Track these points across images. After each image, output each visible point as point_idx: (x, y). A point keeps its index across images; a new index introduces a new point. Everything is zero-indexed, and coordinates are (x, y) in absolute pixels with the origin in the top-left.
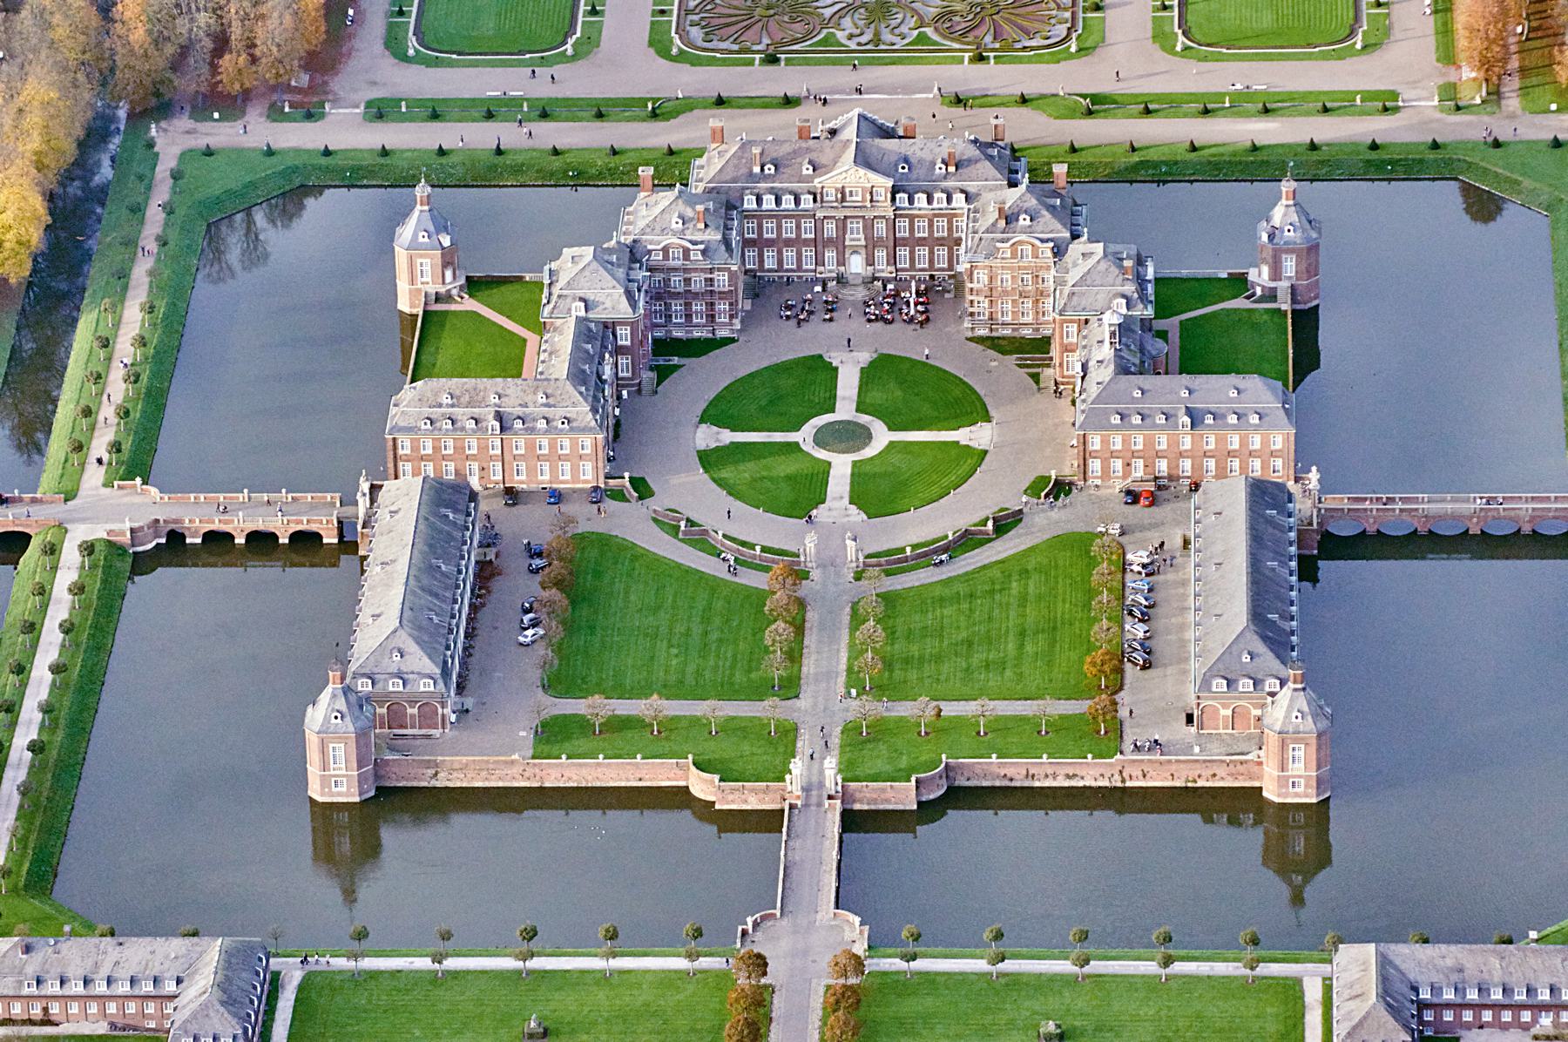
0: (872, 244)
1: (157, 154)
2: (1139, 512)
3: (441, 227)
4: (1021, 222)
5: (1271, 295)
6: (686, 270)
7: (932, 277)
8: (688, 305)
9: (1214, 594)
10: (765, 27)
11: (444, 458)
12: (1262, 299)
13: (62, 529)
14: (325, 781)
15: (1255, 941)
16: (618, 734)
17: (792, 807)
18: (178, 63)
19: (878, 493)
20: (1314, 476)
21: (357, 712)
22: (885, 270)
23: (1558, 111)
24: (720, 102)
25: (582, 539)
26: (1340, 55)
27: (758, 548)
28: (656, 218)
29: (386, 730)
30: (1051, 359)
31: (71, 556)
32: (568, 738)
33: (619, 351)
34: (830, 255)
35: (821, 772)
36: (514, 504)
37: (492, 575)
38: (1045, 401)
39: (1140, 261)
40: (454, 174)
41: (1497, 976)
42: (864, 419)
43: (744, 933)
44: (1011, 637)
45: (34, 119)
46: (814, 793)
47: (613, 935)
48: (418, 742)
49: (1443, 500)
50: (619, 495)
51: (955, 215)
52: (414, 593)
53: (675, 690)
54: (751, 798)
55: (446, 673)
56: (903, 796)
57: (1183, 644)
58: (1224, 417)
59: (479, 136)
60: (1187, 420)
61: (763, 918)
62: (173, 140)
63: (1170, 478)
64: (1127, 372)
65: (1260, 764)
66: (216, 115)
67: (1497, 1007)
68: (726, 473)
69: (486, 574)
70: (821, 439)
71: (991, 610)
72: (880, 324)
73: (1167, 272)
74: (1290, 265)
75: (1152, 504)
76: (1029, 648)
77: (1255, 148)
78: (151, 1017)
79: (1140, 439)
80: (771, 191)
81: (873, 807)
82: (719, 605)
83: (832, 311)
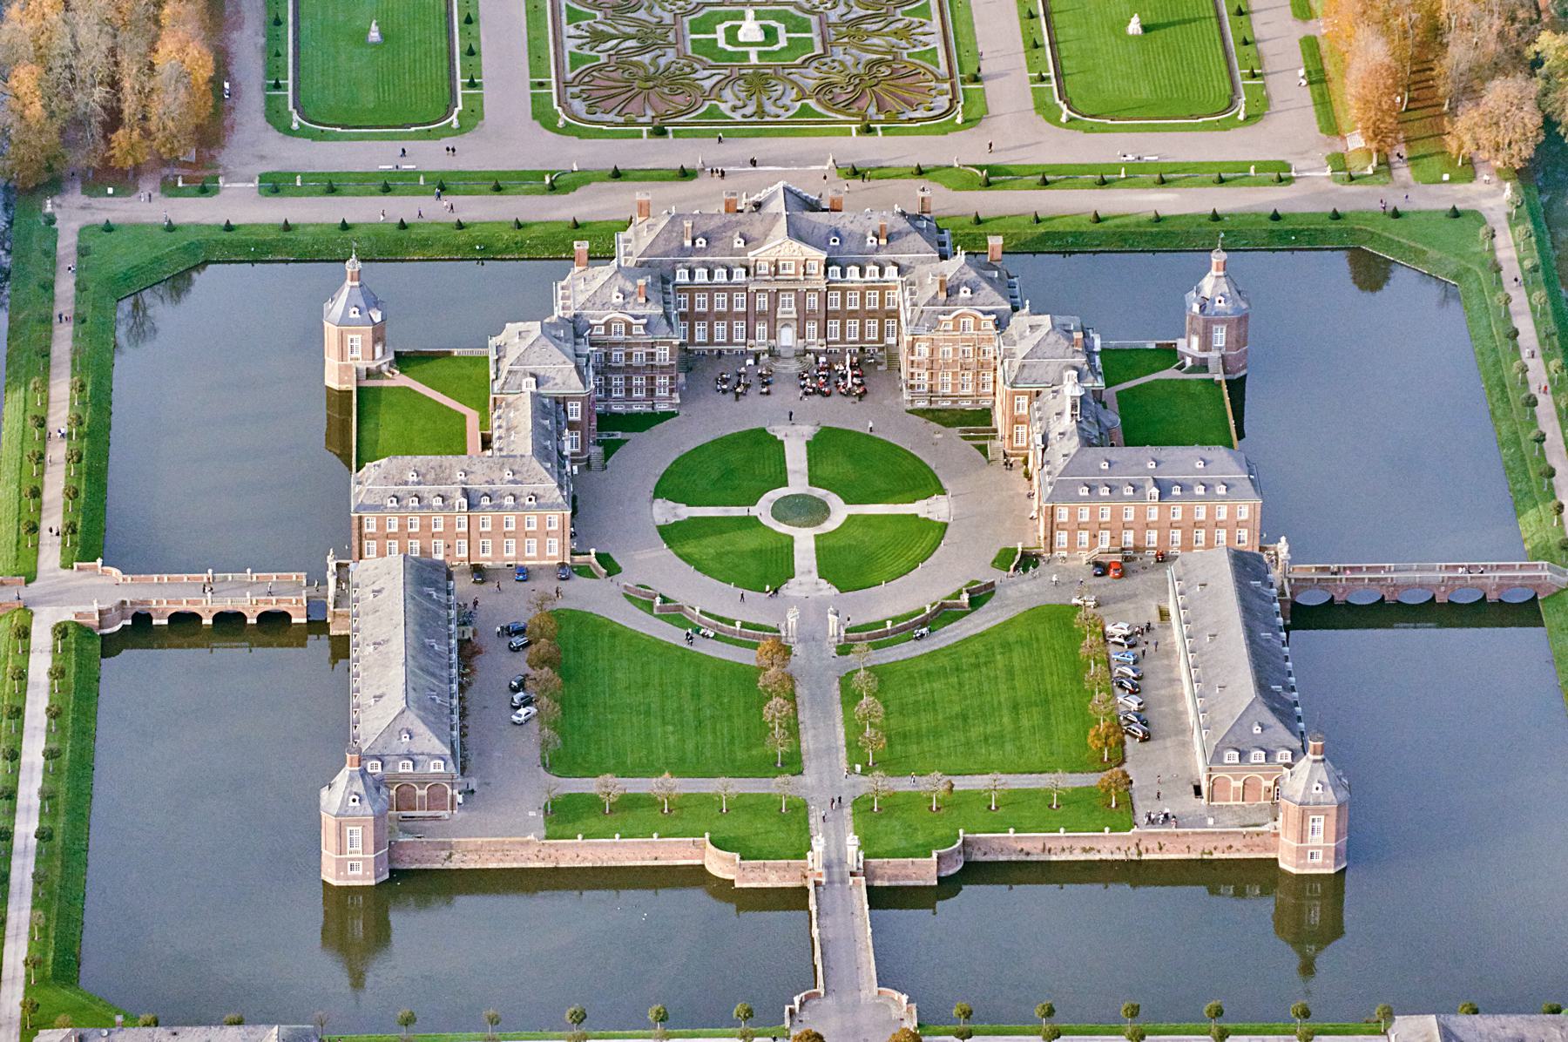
0: (803, 317)
1: (56, 231)
2: (1109, 583)
3: (372, 301)
4: (962, 294)
5: (1202, 366)
6: (628, 345)
7: (862, 349)
8: (628, 379)
10: (647, 98)
12: (1192, 370)
14: (340, 864)
15: (1306, 1014)
16: (631, 813)
17: (817, 884)
19: (846, 566)
20: (1282, 547)
21: (373, 791)
22: (814, 341)
23: (1451, 180)
24: (617, 175)
27: (738, 624)
28: (586, 289)
29: (394, 812)
30: (995, 431)
31: (42, 637)
32: (578, 818)
33: (572, 426)
35: (840, 846)
36: (482, 582)
37: (477, 652)
38: (995, 473)
42: (819, 492)
43: (792, 1012)
44: (1005, 712)
46: (836, 869)
48: (427, 824)
49: (1410, 570)
51: (888, 288)
52: (415, 674)
56: (925, 871)
57: (1179, 716)
58: (1191, 488)
60: (1155, 491)
61: (808, 997)
62: (72, 215)
63: (1136, 549)
64: (1092, 445)
65: (1276, 835)
66: (110, 191)
68: (690, 548)
69: (467, 652)
70: (779, 511)
71: (980, 683)
72: (817, 397)
73: (1113, 343)
74: (1220, 336)
75: (1122, 576)
76: (1025, 723)
77: (1158, 219)
79: (1108, 511)
80: (704, 264)
81: (894, 883)
82: (706, 681)
83: (767, 384)
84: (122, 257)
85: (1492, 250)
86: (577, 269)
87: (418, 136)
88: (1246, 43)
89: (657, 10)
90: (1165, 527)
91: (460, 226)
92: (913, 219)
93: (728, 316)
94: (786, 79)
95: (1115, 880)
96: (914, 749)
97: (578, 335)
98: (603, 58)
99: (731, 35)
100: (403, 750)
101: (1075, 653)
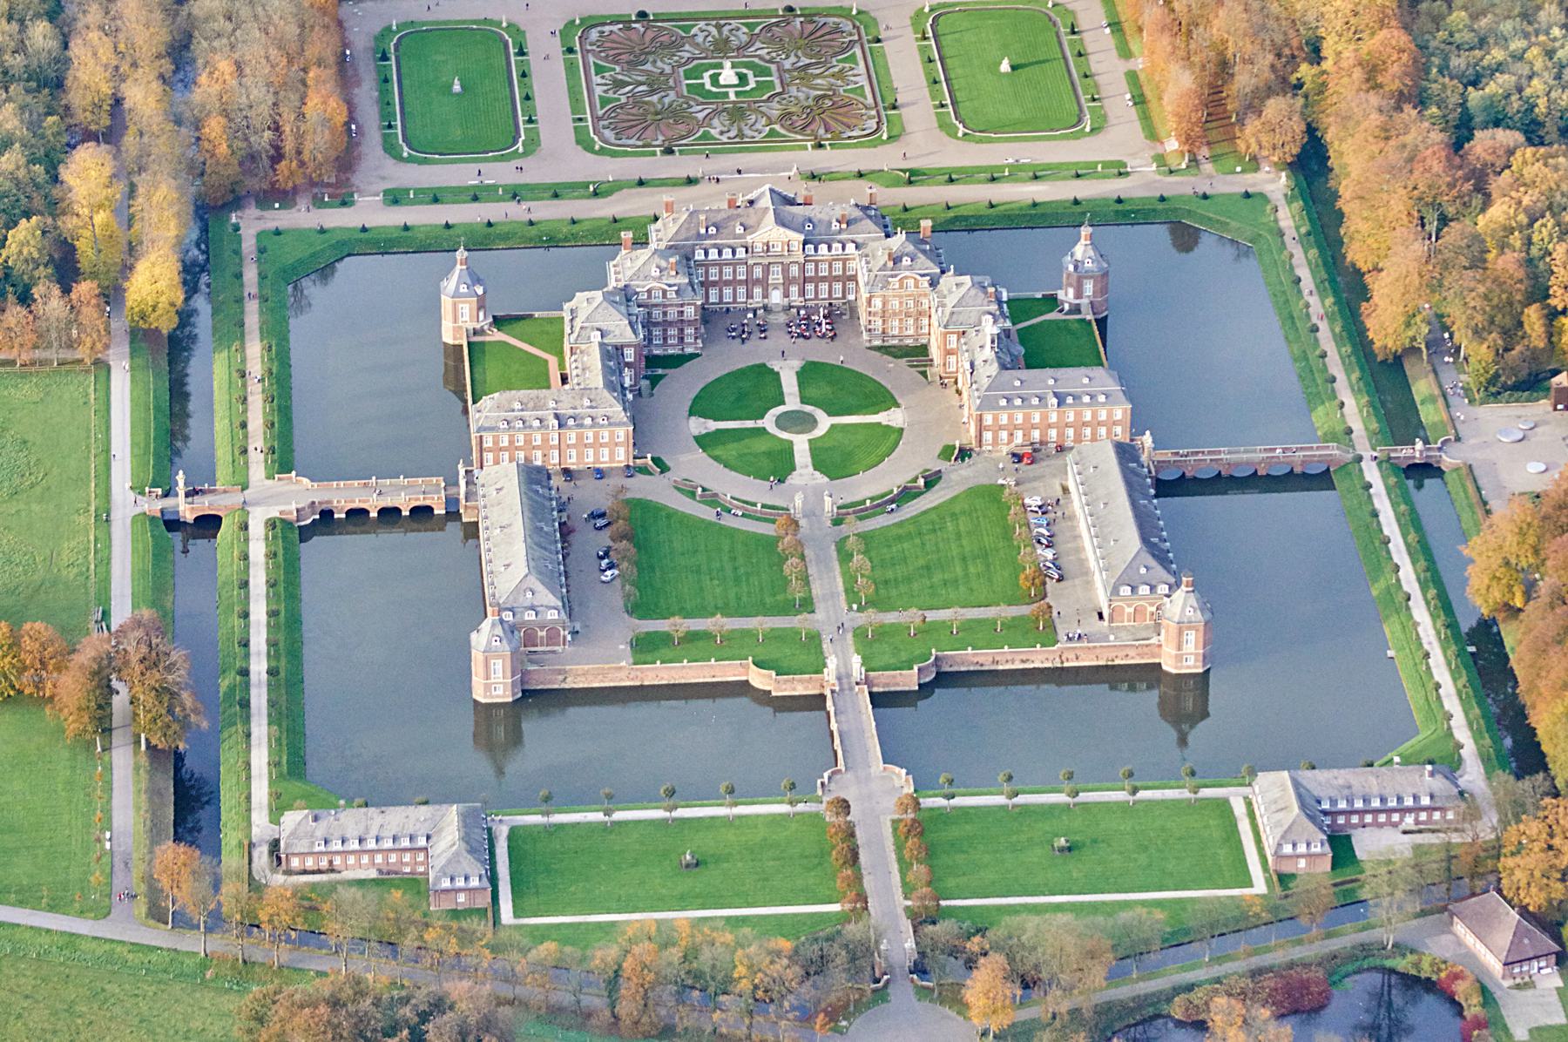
0: (788, 282)
3: (478, 281)
5: (1076, 309)
6: (665, 306)
8: (665, 331)
9: (1099, 525)
11: (517, 448)
12: (1070, 312)
14: (487, 687)
15: (1193, 774)
17: (833, 692)
19: (835, 461)
20: (1147, 439)
22: (795, 299)
24: (641, 183)
28: (627, 267)
31: (257, 529)
34: (758, 291)
35: (846, 663)
37: (571, 532)
38: (935, 390)
40: (483, 240)
41: (1375, 790)
42: (808, 408)
47: (731, 791)
50: (644, 470)
54: (799, 687)
56: (909, 680)
57: (1082, 562)
60: (1055, 401)
61: (833, 773)
62: (251, 224)
63: (1041, 443)
67: (1376, 812)
68: (717, 452)
74: (1089, 287)
76: (972, 570)
77: (1035, 205)
78: (407, 864)
80: (715, 246)
84: (292, 253)
85: (1276, 221)
86: (624, 252)
87: (495, 159)
88: (1086, 76)
89: (659, 64)
90: (1062, 426)
91: (531, 223)
92: (865, 209)
93: (734, 283)
94: (757, 111)
95: (1047, 682)
96: (894, 592)
97: (628, 300)
98: (623, 100)
99: (715, 79)
100: (527, 604)
101: (1004, 518)
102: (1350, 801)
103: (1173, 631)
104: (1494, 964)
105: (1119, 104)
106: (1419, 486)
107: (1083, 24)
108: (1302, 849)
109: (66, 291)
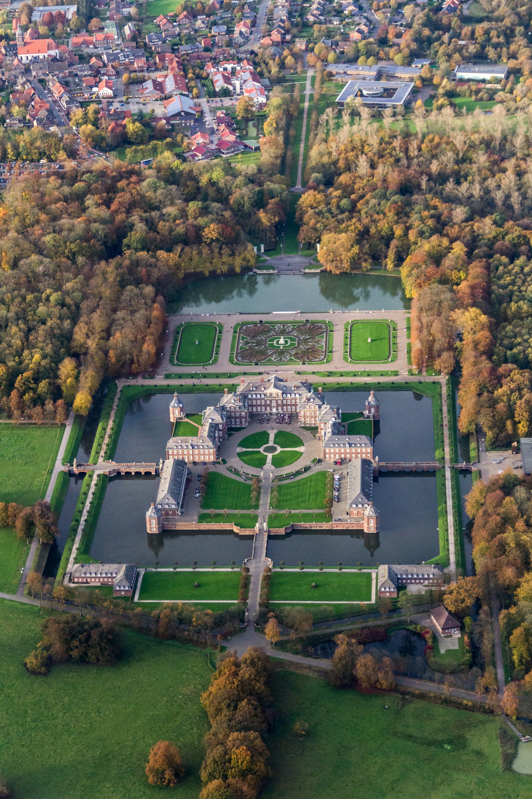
2: (338, 467)
5: (368, 417)
9: (353, 486)
13: (93, 471)
14: (151, 528)
16: (217, 517)
18: (122, 366)
19: (278, 462)
20: (377, 458)
22: (280, 411)
24: (245, 374)
25: (211, 474)
26: (385, 363)
31: (95, 477)
38: (316, 441)
39: (338, 409)
40: (182, 390)
45: (89, 379)
47: (215, 563)
50: (219, 463)
53: (229, 508)
54: (247, 532)
55: (178, 504)
56: (282, 531)
59: (189, 382)
62: (121, 384)
67: (415, 579)
68: (244, 458)
70: (265, 451)
74: (373, 410)
93: (261, 405)
99: (277, 342)
102: (407, 575)
103: (366, 519)
104: (439, 628)
105: (402, 354)
106: (465, 477)
107: (399, 327)
108: (388, 590)
109: (55, 402)
